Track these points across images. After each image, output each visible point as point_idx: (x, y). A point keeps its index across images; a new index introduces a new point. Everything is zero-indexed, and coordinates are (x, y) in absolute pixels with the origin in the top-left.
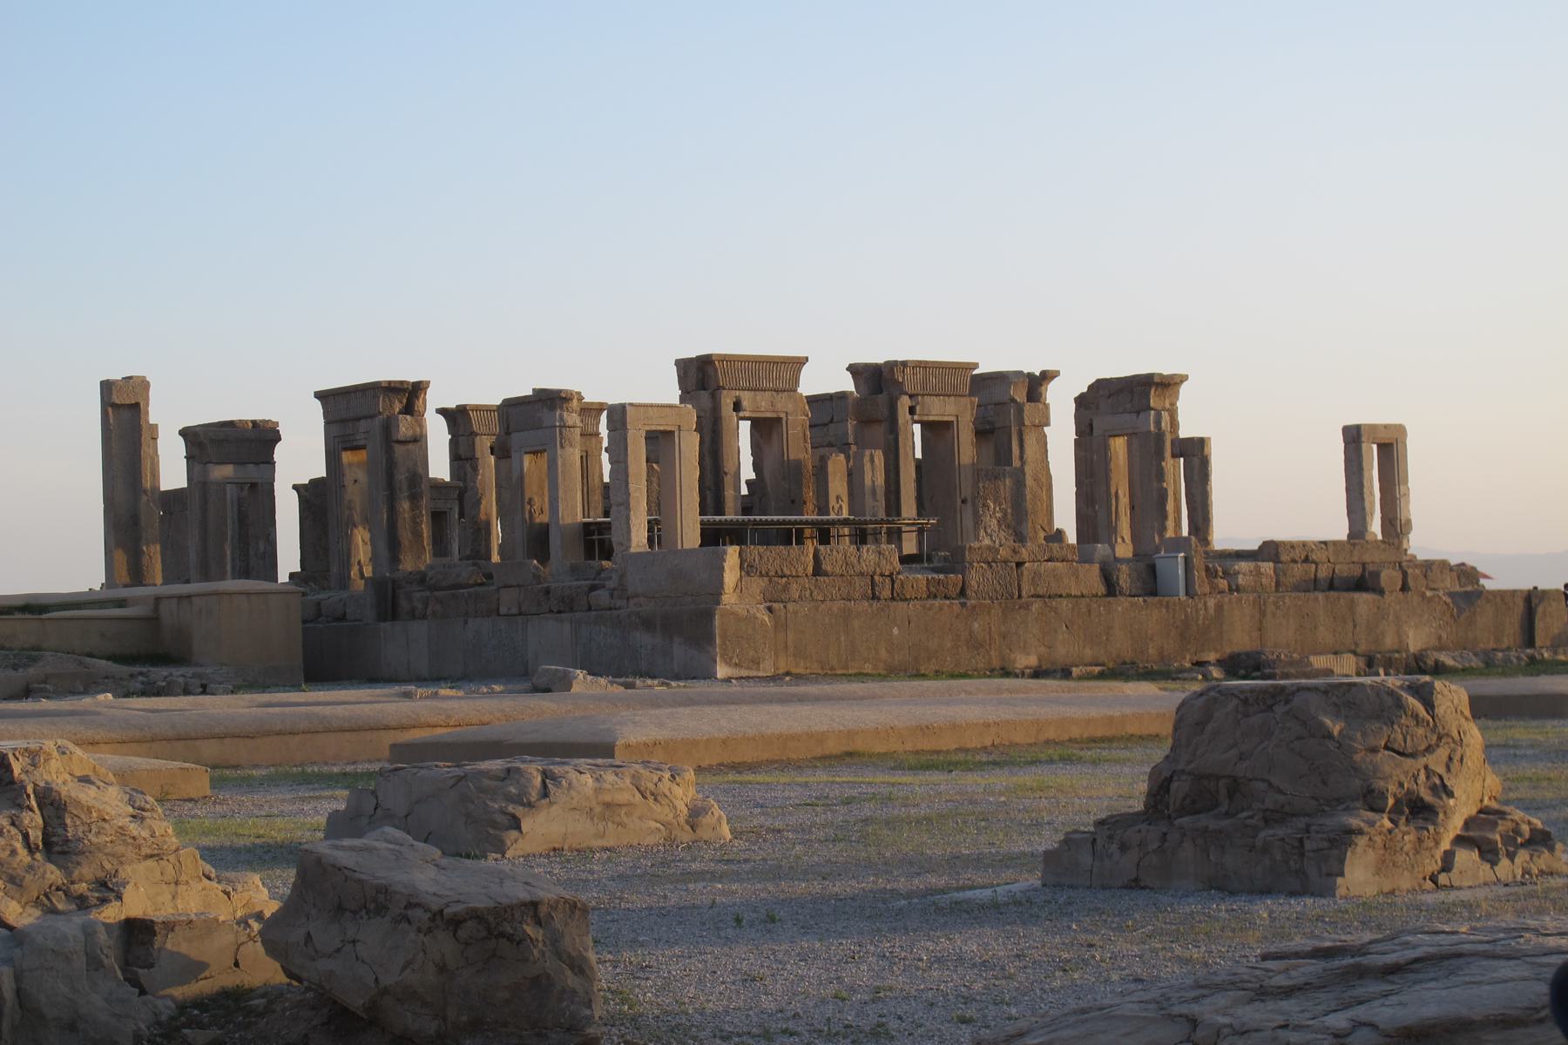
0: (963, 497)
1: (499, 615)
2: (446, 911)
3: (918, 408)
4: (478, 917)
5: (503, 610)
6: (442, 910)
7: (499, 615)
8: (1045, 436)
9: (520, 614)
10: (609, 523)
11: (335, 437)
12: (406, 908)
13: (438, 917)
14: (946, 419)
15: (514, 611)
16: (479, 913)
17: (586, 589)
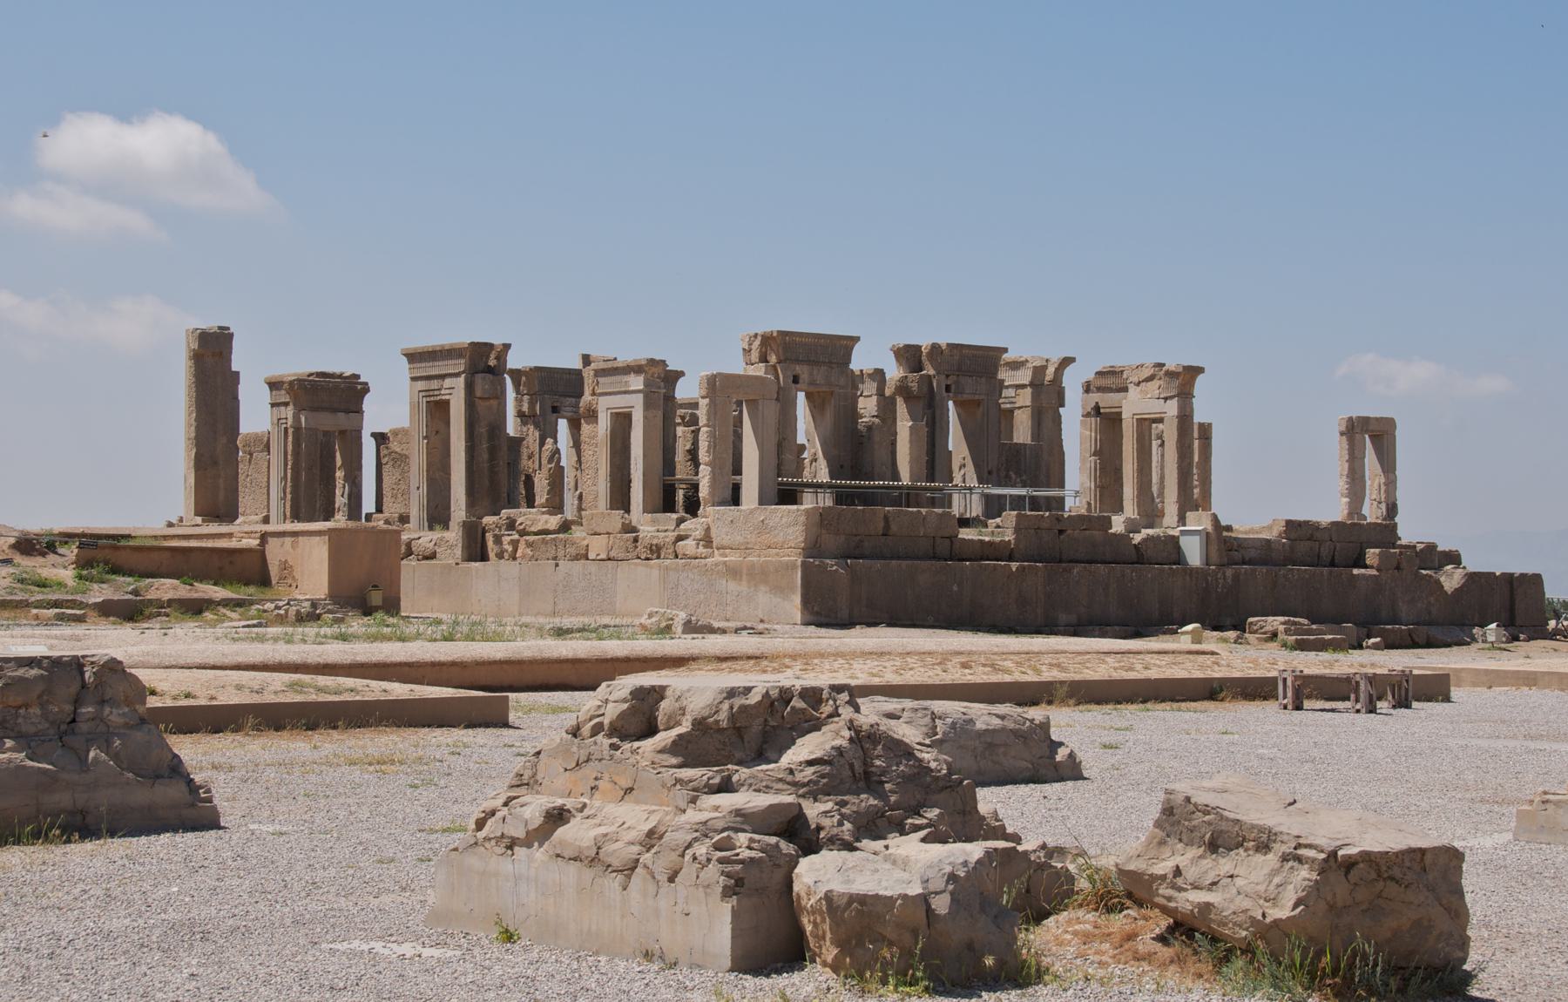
0: (990, 468)
1: (588, 559)
2: (1340, 853)
3: (953, 387)
4: (1371, 861)
5: (592, 555)
6: (1336, 853)
7: (588, 559)
8: (1060, 416)
9: (609, 559)
10: (733, 475)
11: (420, 391)
12: (1295, 848)
13: (1332, 860)
14: (977, 397)
15: (603, 556)
16: (1373, 858)
17: (673, 539)
